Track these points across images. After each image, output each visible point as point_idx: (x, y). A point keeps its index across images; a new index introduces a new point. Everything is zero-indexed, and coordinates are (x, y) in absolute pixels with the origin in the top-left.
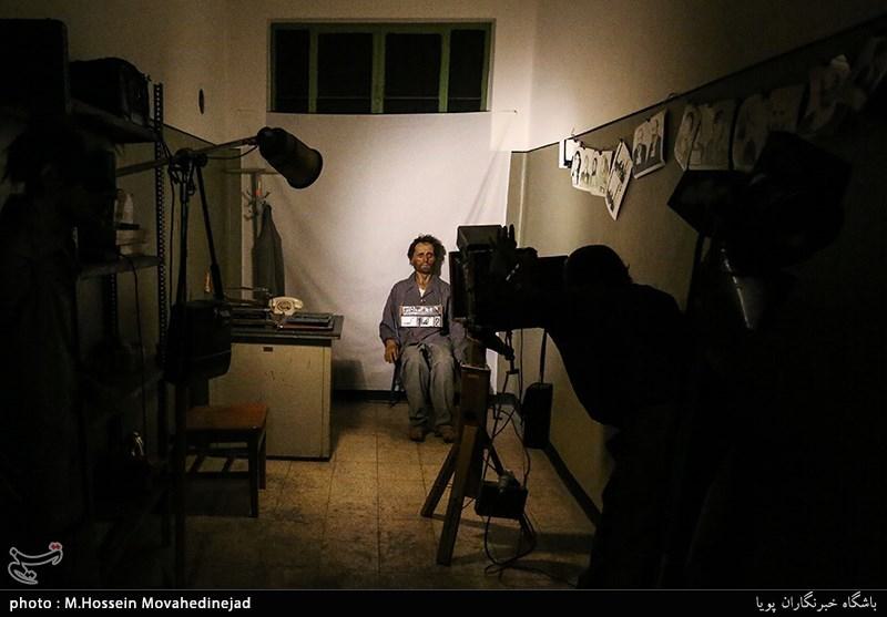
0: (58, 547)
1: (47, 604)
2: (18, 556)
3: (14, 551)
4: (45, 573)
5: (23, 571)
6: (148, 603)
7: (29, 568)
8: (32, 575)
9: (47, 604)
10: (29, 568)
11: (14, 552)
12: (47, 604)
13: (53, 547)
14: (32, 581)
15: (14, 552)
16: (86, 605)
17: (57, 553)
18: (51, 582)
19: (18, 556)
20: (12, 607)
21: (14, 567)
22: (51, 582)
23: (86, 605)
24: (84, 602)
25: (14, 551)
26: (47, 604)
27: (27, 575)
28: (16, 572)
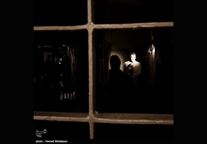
2: (38, 132)
3: (37, 131)
4: (43, 135)
5: (39, 135)
6: (56, 141)
7: (40, 134)
9: (41, 141)
12: (41, 141)
14: (41, 137)
16: (46, 142)
18: (44, 137)
19: (38, 132)
21: (37, 134)
22: (44, 137)
23: (46, 142)
24: (46, 141)
25: (37, 131)
27: (40, 135)
28: (37, 135)
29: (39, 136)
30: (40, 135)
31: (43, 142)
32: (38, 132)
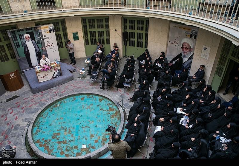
0: (15, 147)
1: (11, 162)
2: (5, 150)
5: (6, 154)
7: (8, 153)
8: (8, 155)
10: (8, 153)
11: (3, 148)
13: (14, 147)
14: (8, 157)
15: (3, 148)
17: (15, 149)
20: (3, 163)
21: (3, 153)
26: (11, 162)
27: (7, 155)
28: (4, 154)
29: (6, 155)
30: (7, 155)
31: (13, 163)
32: (5, 150)
